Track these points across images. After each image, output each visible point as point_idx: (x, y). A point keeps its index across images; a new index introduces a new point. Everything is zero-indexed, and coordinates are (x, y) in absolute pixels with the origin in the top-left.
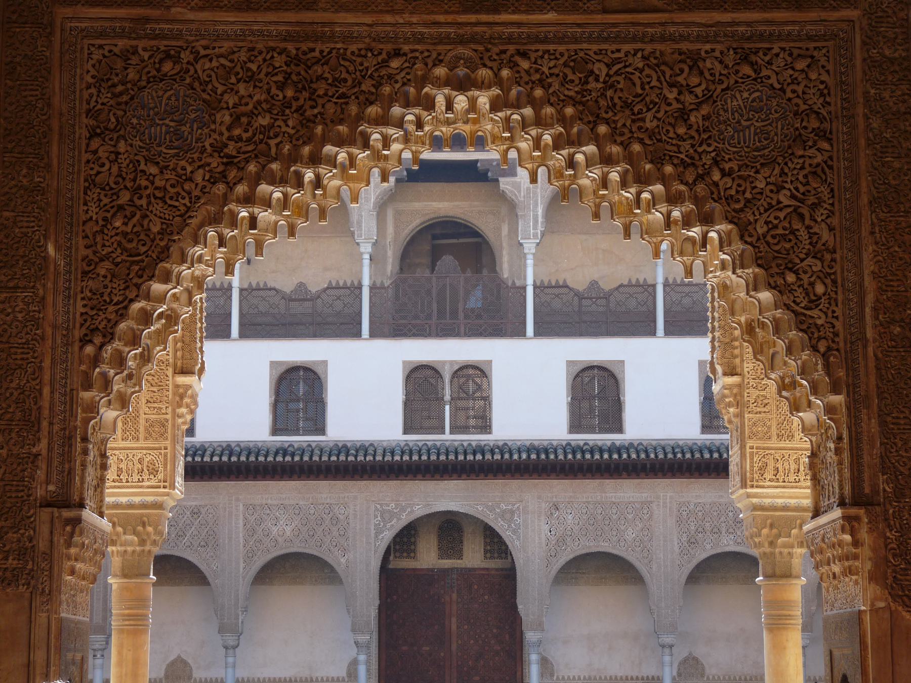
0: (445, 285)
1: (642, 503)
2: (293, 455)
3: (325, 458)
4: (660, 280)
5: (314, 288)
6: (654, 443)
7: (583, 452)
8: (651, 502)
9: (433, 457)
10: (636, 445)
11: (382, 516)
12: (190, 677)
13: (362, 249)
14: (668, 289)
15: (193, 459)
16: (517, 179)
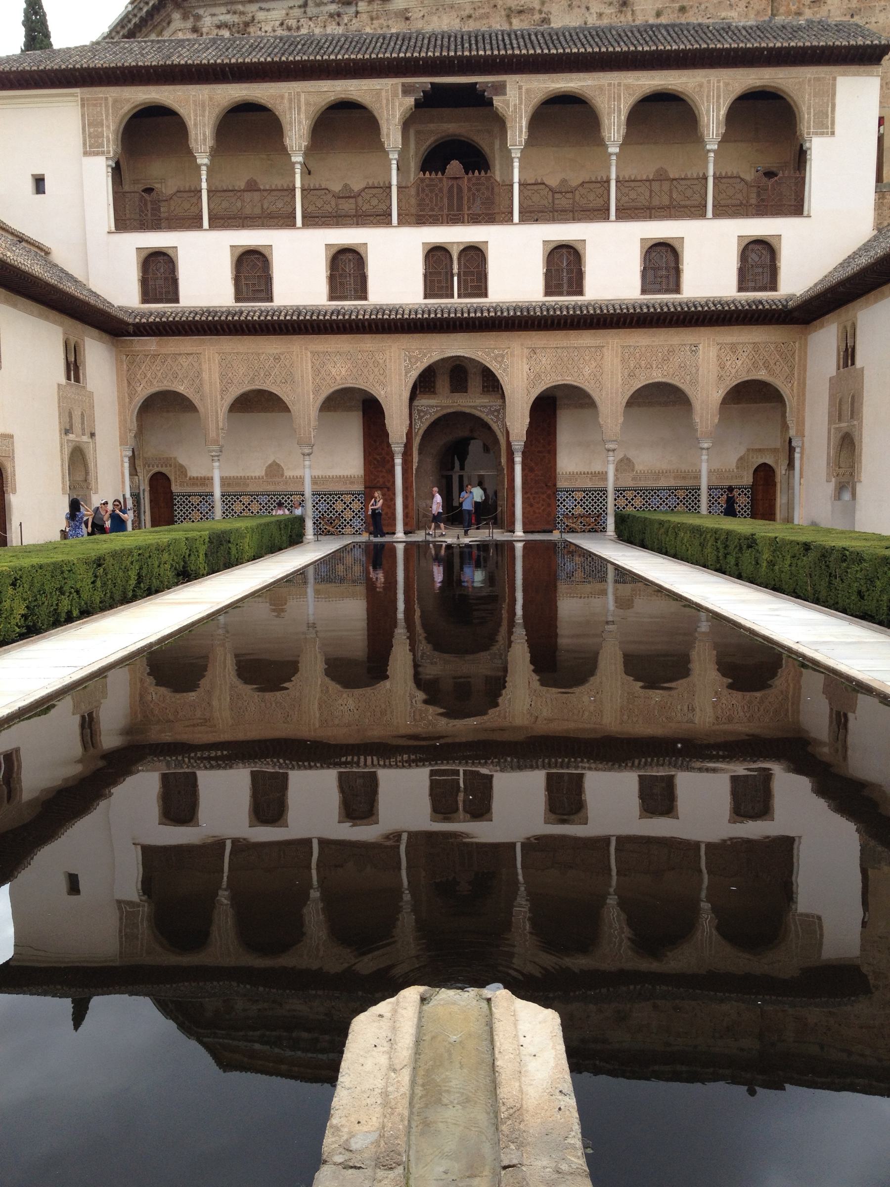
0: (452, 185)
1: (596, 347)
2: (344, 315)
3: (367, 317)
4: (613, 176)
5: (357, 186)
6: (606, 302)
7: (555, 310)
8: (603, 347)
9: (446, 315)
10: (593, 303)
11: (410, 360)
12: (282, 475)
13: (391, 156)
14: (619, 184)
15: (272, 318)
16: (507, 97)
